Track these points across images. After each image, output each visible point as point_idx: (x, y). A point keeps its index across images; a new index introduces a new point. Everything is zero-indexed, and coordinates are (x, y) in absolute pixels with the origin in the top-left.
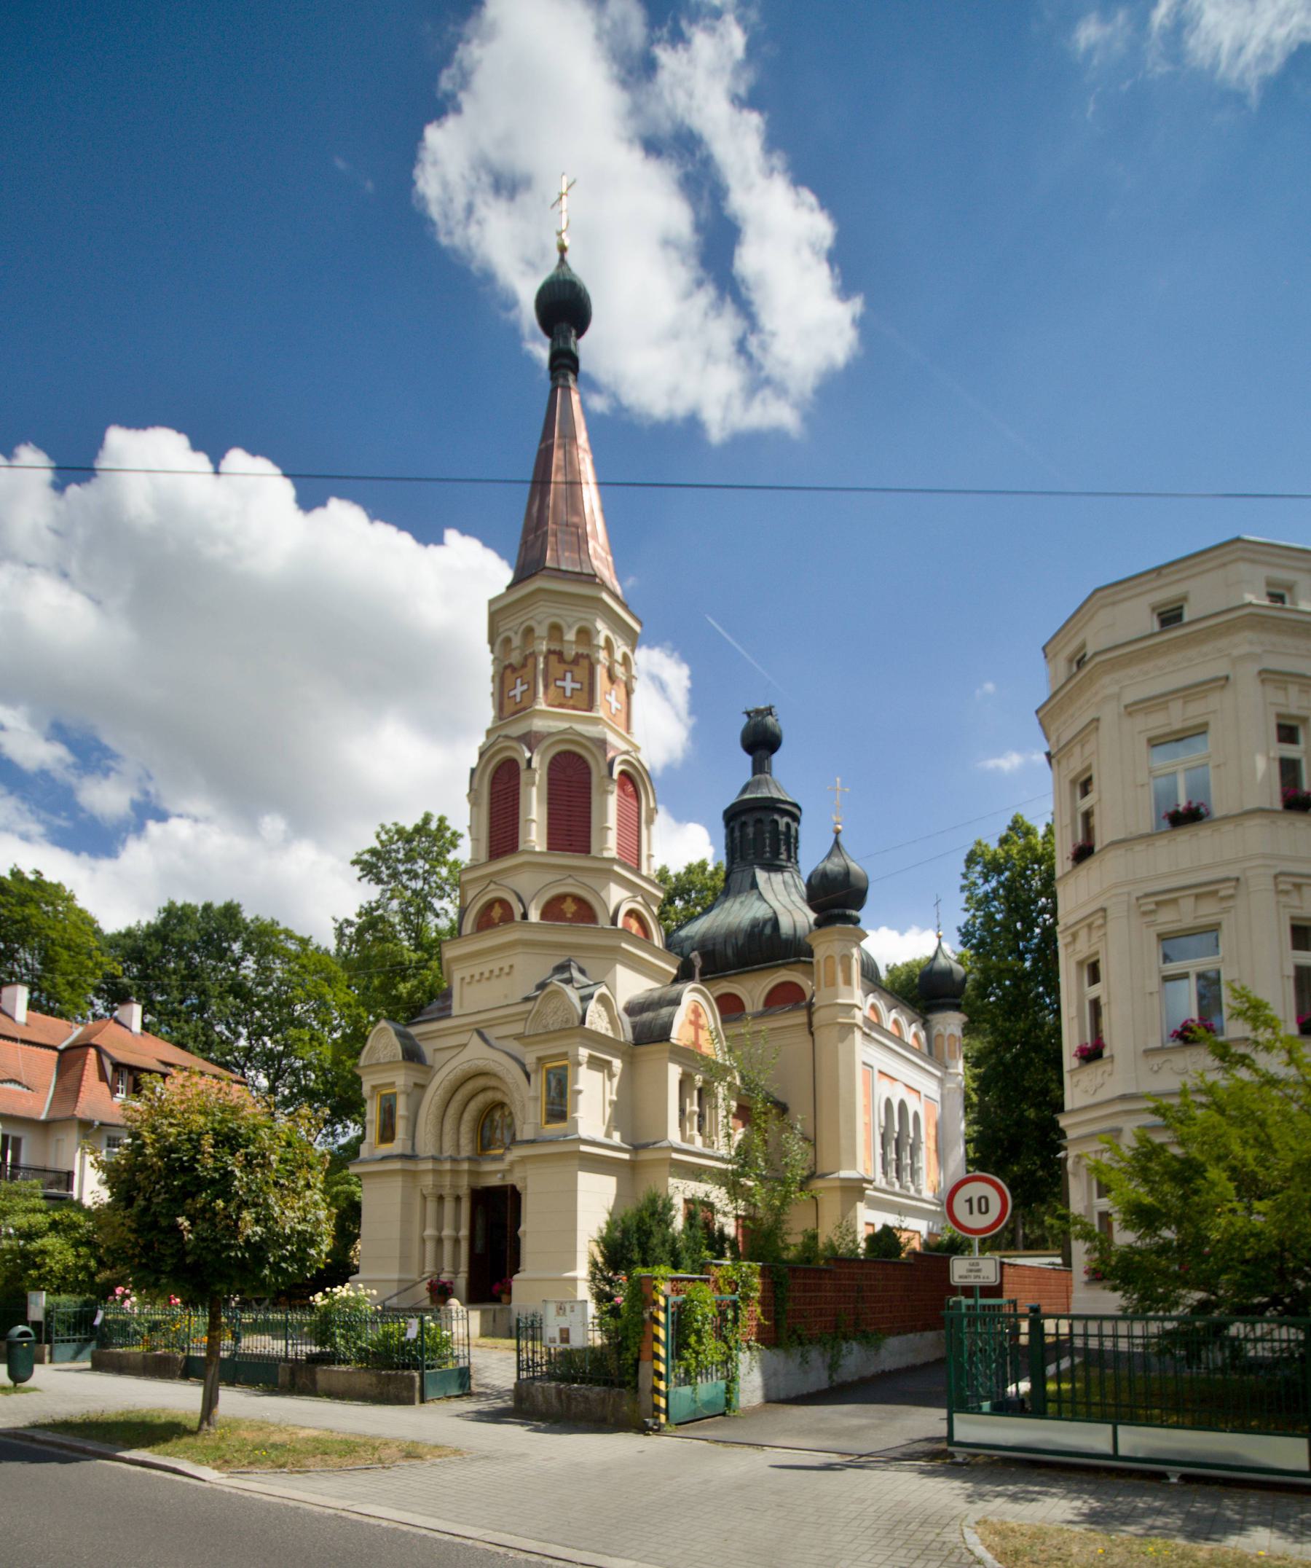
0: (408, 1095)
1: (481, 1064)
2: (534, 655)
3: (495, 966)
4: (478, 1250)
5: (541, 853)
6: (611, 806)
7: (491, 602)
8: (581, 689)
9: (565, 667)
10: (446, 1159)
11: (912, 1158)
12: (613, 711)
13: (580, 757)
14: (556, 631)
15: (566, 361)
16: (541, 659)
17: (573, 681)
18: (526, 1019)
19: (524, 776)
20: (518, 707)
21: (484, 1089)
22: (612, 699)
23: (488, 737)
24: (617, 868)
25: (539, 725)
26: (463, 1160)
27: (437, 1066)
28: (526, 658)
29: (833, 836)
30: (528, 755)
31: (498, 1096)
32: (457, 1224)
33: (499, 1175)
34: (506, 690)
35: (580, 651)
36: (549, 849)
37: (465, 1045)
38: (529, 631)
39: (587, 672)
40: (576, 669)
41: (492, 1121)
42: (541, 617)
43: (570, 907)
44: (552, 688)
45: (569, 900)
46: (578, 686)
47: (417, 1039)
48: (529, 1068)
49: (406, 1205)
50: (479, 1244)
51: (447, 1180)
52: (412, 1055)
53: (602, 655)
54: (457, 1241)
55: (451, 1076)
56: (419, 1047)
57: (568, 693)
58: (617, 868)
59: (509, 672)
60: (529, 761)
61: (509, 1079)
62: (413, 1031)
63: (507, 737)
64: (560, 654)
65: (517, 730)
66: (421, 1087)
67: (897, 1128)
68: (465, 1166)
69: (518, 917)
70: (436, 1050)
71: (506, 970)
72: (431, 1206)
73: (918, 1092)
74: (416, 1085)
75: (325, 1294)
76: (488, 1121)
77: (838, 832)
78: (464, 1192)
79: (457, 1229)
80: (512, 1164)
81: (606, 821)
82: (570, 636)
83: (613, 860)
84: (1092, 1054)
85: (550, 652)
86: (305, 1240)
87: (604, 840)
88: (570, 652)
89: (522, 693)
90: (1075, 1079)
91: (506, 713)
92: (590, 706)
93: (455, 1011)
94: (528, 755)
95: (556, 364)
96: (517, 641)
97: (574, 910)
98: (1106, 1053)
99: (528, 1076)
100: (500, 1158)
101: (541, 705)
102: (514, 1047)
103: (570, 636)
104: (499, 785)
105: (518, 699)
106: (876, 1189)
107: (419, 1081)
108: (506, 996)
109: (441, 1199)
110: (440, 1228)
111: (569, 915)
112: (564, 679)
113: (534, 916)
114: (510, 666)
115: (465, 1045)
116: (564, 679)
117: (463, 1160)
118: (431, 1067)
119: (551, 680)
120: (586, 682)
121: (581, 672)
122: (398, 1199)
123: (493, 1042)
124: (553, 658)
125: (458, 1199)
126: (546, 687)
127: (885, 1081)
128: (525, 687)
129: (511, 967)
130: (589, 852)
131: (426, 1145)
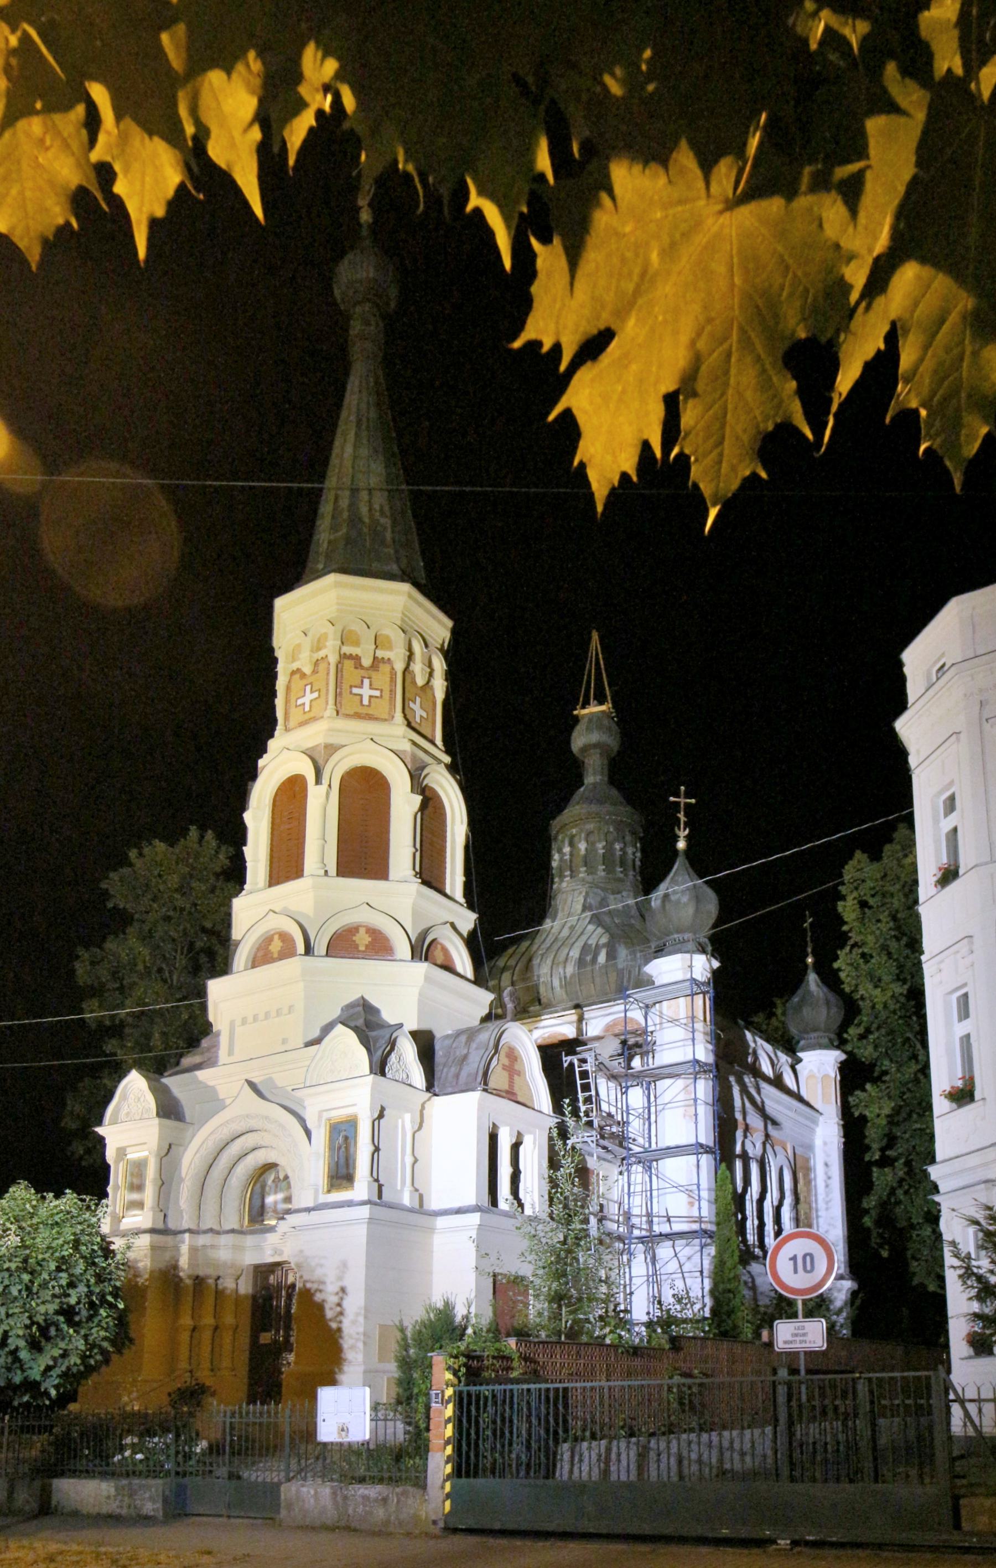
9: (362, 672)
20: (307, 716)
28: (317, 663)
34: (293, 699)
39: (388, 679)
40: (374, 674)
57: (366, 702)
111: (362, 948)
112: (361, 686)
116: (361, 686)
119: (345, 687)
124: (348, 664)
128: (316, 695)
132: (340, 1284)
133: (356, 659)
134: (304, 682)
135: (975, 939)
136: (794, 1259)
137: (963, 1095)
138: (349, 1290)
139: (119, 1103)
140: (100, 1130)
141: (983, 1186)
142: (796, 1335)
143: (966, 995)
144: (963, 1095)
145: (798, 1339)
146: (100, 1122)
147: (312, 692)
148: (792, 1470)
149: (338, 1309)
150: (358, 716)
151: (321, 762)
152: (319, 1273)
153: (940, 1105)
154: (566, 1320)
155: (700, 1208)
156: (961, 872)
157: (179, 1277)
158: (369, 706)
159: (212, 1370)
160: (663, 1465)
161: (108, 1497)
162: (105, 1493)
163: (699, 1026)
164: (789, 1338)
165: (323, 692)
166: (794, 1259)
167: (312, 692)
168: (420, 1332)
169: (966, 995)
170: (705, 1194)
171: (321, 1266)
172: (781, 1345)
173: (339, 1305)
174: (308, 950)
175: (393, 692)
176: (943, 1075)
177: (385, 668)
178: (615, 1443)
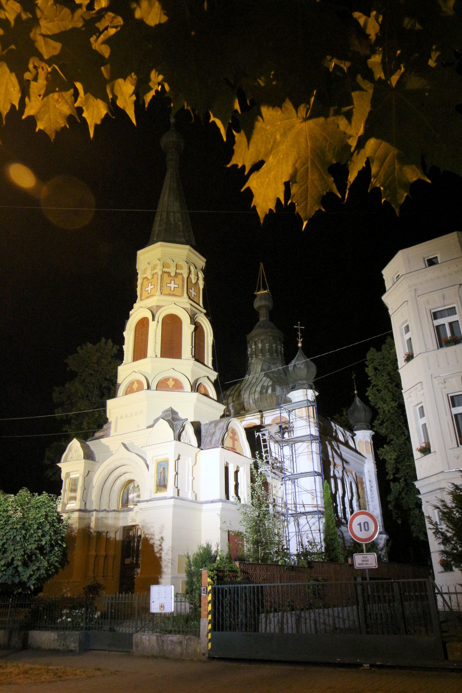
9: (171, 278)
39: (181, 281)
40: (176, 279)
57: (172, 289)
69: (145, 387)
112: (171, 283)
113: (153, 386)
116: (171, 283)
119: (164, 284)
128: (153, 287)
132: (161, 535)
133: (169, 273)
134: (149, 282)
135: (423, 383)
136: (360, 524)
137: (426, 450)
138: (165, 538)
139: (68, 452)
140: (59, 465)
141: (439, 491)
142: (363, 561)
143: (422, 407)
144: (426, 450)
145: (365, 563)
146: (59, 461)
147: (151, 285)
148: (367, 628)
149: (160, 547)
150: (169, 295)
151: (154, 312)
152: (151, 530)
153: (417, 455)
154: (261, 554)
155: (317, 501)
156: (414, 356)
157: (90, 532)
158: (174, 291)
159: (104, 577)
160: (308, 625)
161: (54, 640)
162: (53, 638)
163: (312, 420)
164: (361, 562)
166: (360, 524)
167: (151, 285)
168: (196, 559)
169: (422, 407)
170: (319, 494)
171: (153, 527)
172: (357, 566)
173: (160, 545)
174: (149, 387)
175: (183, 286)
176: (416, 442)
177: (180, 277)
178: (285, 614)
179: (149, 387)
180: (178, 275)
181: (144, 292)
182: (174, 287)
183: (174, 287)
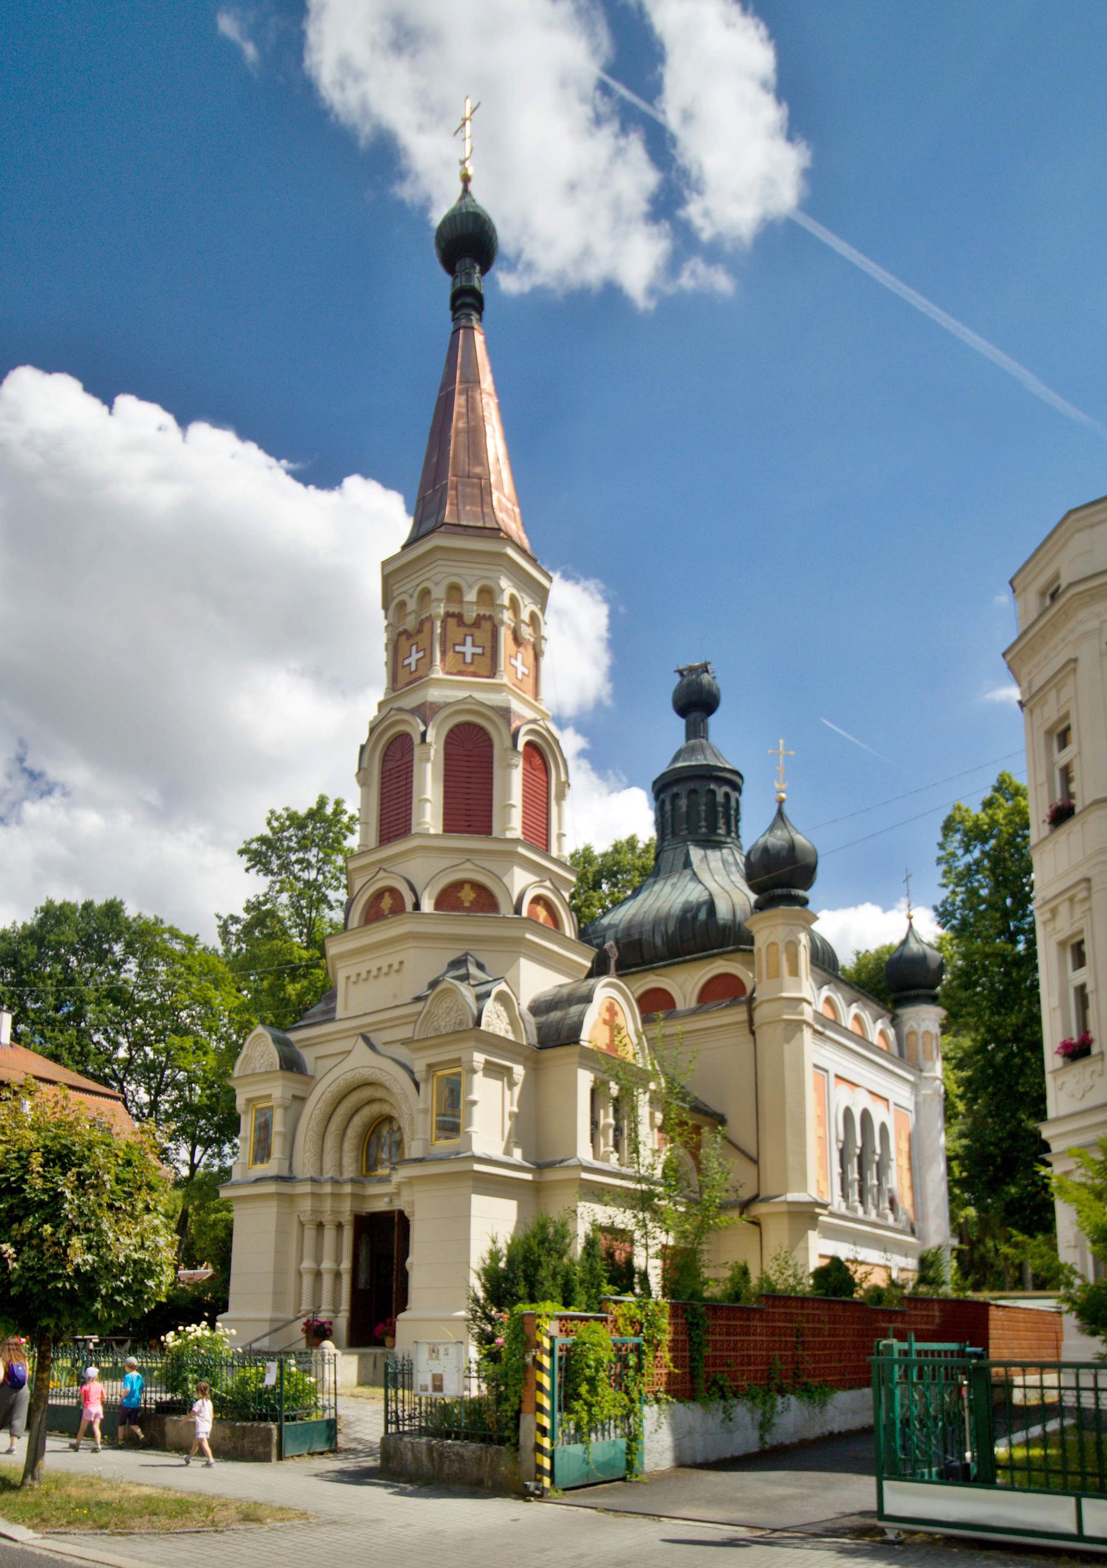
0: (286, 1109)
1: (366, 1073)
2: (430, 619)
3: (384, 963)
4: (362, 1284)
5: (436, 836)
6: (513, 784)
7: (385, 564)
8: (483, 654)
9: (464, 630)
10: (326, 1181)
11: (878, 1179)
12: (520, 676)
13: (481, 729)
14: (455, 591)
15: (469, 300)
16: (438, 624)
17: (474, 645)
18: (415, 1022)
19: (418, 751)
21: (371, 1101)
22: (518, 663)
23: (379, 711)
24: (521, 850)
25: (434, 695)
26: (345, 1182)
27: (318, 1076)
28: (422, 623)
29: (776, 805)
30: (422, 728)
31: (386, 1109)
32: (338, 1257)
33: (386, 1199)
34: (400, 659)
35: (482, 613)
36: (445, 831)
37: (349, 1052)
38: (426, 593)
39: (489, 634)
40: (477, 633)
41: (379, 1138)
42: (438, 576)
43: (468, 895)
44: (450, 654)
45: (467, 887)
46: (479, 651)
47: (297, 1046)
48: (418, 1077)
49: (281, 1232)
50: (363, 1278)
51: (328, 1205)
52: (291, 1063)
53: (507, 616)
54: (338, 1275)
55: (333, 1087)
56: (299, 1056)
57: (468, 659)
58: (521, 850)
59: (404, 637)
60: (424, 735)
61: (396, 1089)
62: (293, 1036)
63: (400, 710)
64: (459, 617)
65: (411, 701)
66: (301, 1100)
67: (859, 1143)
68: (348, 1189)
69: (409, 907)
70: (317, 1058)
71: (396, 967)
72: (310, 1233)
73: (887, 1100)
74: (294, 1097)
75: (178, 1333)
76: (374, 1137)
77: (781, 802)
78: (347, 1218)
79: (338, 1260)
80: (400, 1185)
81: (509, 798)
82: (471, 596)
83: (516, 841)
84: (1077, 1051)
85: (448, 615)
86: (142, 1270)
87: (507, 818)
88: (471, 614)
89: (417, 660)
90: (1059, 1081)
91: (399, 685)
92: (493, 672)
93: (340, 1013)
94: (422, 728)
95: (459, 303)
96: (412, 605)
97: (471, 899)
98: (1095, 1049)
99: (417, 1085)
100: (386, 1180)
101: (438, 673)
102: (402, 1053)
103: (471, 596)
104: (389, 762)
105: (413, 668)
106: (832, 1215)
107: (297, 1093)
108: (395, 996)
109: (320, 1226)
110: (318, 1260)
112: (464, 644)
113: (427, 906)
114: (405, 632)
115: (349, 1052)
116: (464, 644)
117: (345, 1182)
118: (313, 1077)
119: (449, 645)
120: (488, 645)
121: (483, 635)
122: (272, 1227)
123: (380, 1047)
124: (452, 622)
125: (339, 1226)
126: (444, 653)
127: (844, 1087)
128: (421, 654)
129: (401, 963)
130: (490, 833)
131: (304, 1166)
134: (412, 641)
165: (428, 653)
179: (417, 906)
180: (483, 622)
181: (400, 671)
182: (473, 654)
183: (473, 654)
